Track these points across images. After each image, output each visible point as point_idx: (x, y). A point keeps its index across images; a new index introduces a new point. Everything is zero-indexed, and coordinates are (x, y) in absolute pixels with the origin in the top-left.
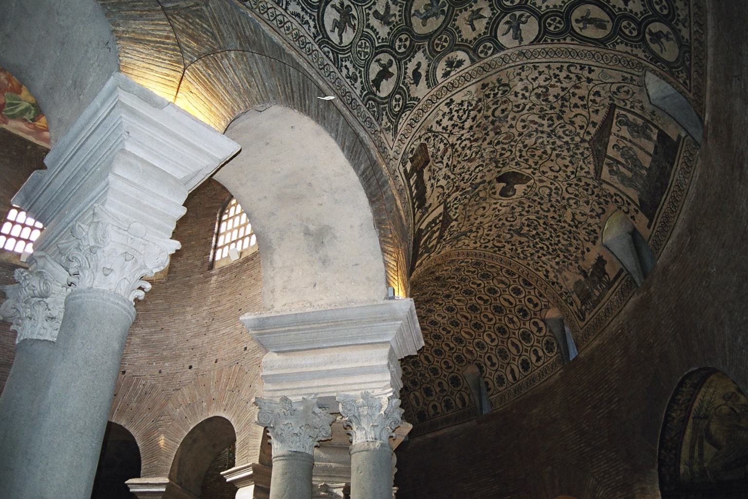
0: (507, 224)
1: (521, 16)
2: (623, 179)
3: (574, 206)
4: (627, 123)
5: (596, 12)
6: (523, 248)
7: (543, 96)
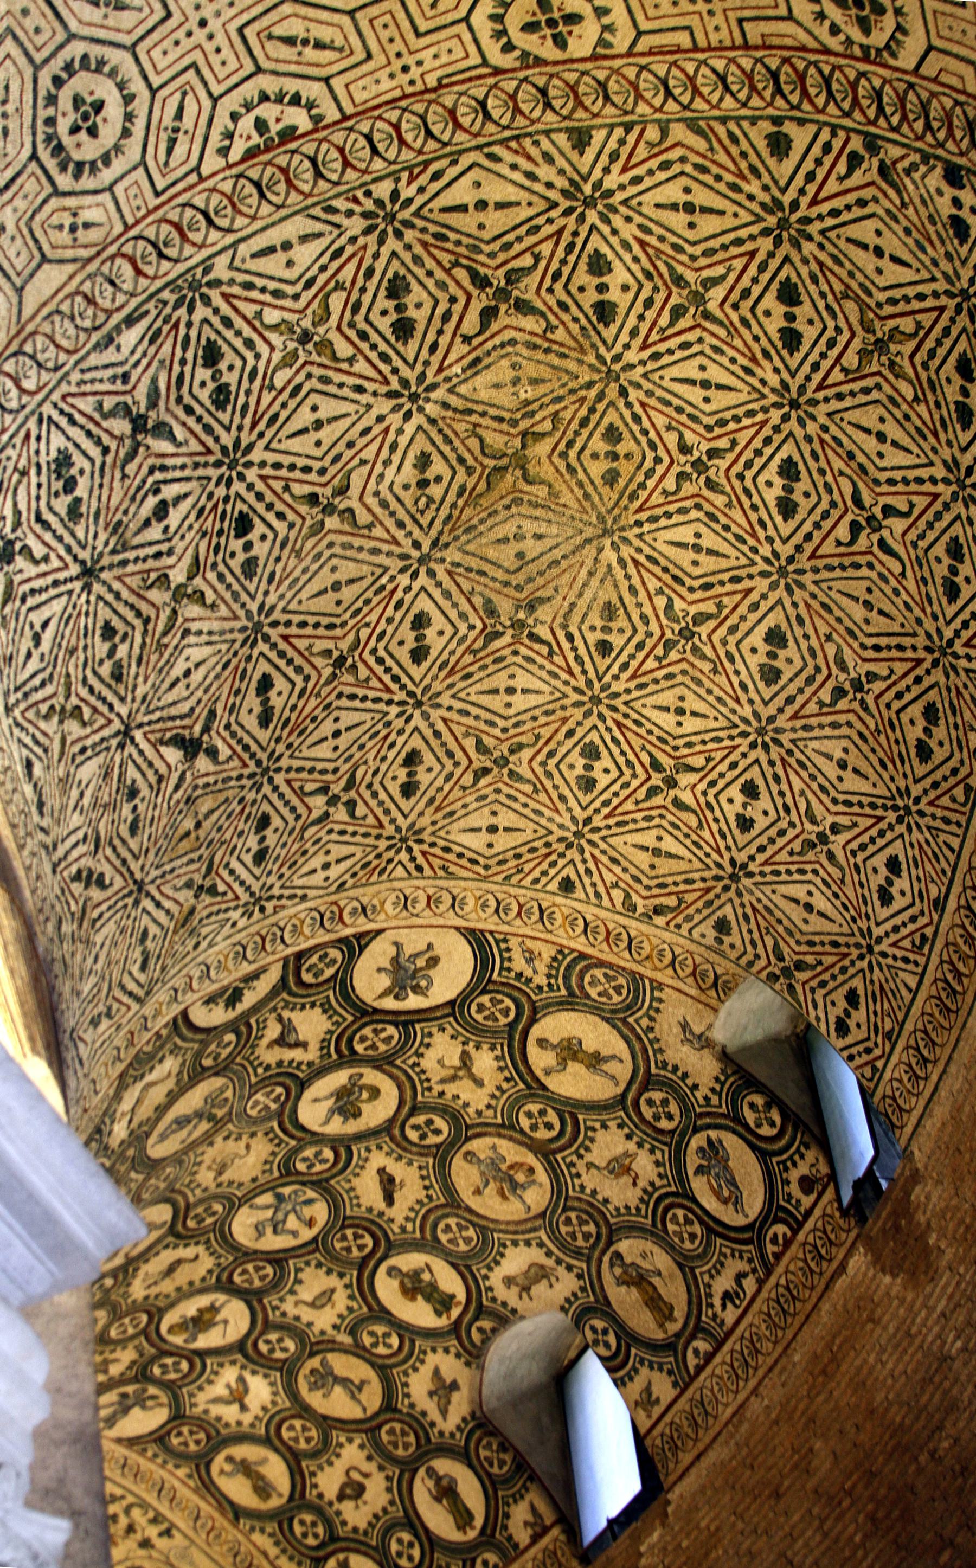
1: (153, 1397)
5: (276, 1471)
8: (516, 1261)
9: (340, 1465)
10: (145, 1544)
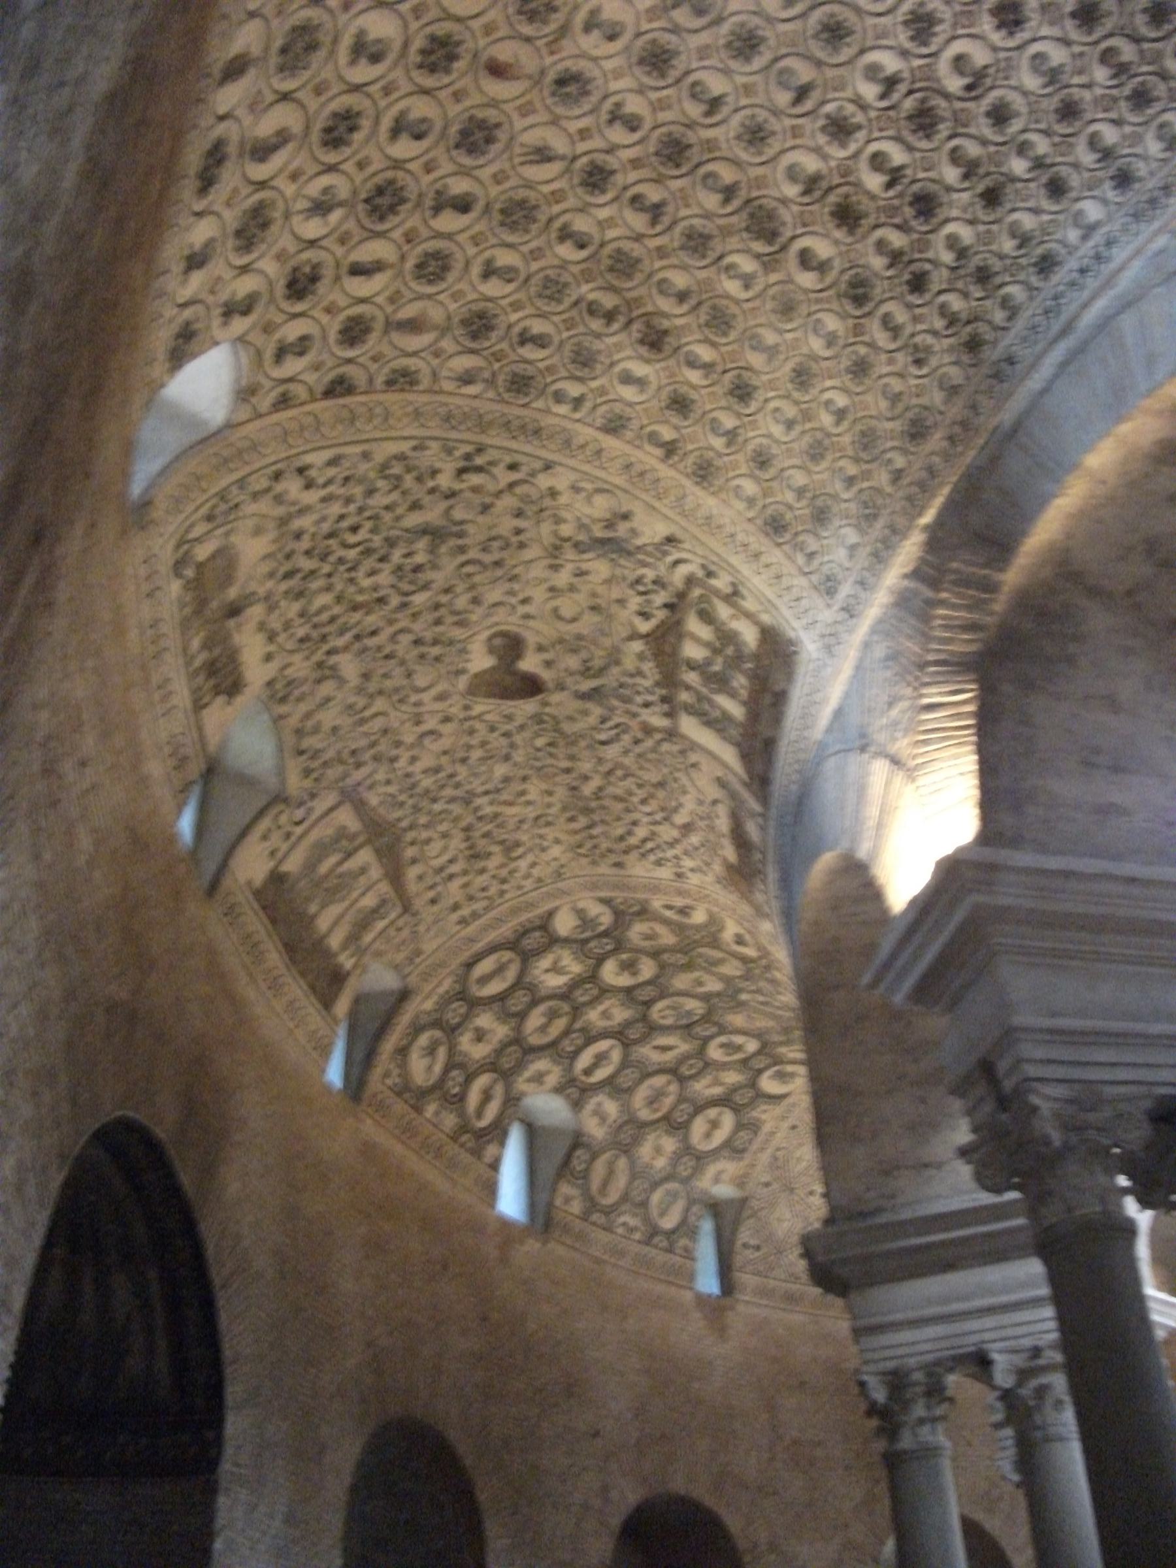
0: (472, 554)
2: (321, 850)
3: (352, 699)
4: (375, 913)
5: (494, 988)
6: (404, 493)
7: (509, 848)
8: (611, 1108)
9: (495, 1025)
10: (456, 907)
